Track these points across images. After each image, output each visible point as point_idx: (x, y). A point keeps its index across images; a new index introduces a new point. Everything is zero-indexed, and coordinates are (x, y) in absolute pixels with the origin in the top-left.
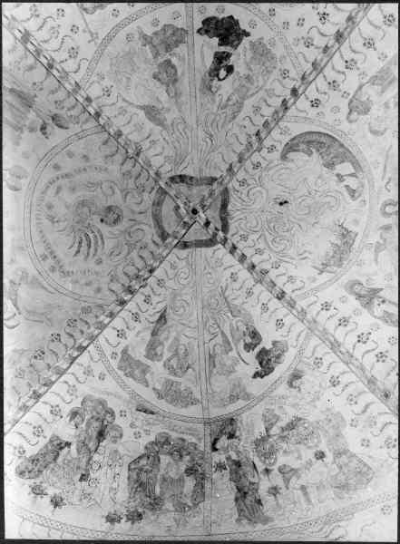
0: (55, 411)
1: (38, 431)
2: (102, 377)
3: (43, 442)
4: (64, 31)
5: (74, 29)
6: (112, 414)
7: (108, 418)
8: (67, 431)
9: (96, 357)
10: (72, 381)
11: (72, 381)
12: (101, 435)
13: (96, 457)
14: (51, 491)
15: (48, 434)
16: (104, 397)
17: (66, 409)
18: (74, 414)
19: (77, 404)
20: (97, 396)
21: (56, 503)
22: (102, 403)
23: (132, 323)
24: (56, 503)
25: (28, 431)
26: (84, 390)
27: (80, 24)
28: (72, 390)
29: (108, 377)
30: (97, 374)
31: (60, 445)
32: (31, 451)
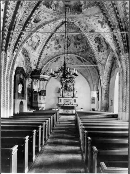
0: (94, 45)
1: (96, 48)
2: (92, 36)
3: (97, 48)
4: (43, 40)
5: (43, 38)
6: (98, 37)
7: (98, 38)
8: (97, 44)
9: (89, 37)
10: (91, 41)
11: (91, 41)
12: (100, 41)
13: (102, 43)
14: (102, 51)
15: (96, 47)
16: (95, 37)
17: (95, 43)
18: (96, 42)
19: (95, 42)
20: (95, 38)
21: (103, 51)
22: (96, 38)
23: (86, 30)
24: (103, 51)
25: (95, 49)
26: (93, 40)
27: (42, 38)
28: (93, 42)
29: (93, 35)
30: (92, 37)
31: (98, 46)
32: (97, 50)
